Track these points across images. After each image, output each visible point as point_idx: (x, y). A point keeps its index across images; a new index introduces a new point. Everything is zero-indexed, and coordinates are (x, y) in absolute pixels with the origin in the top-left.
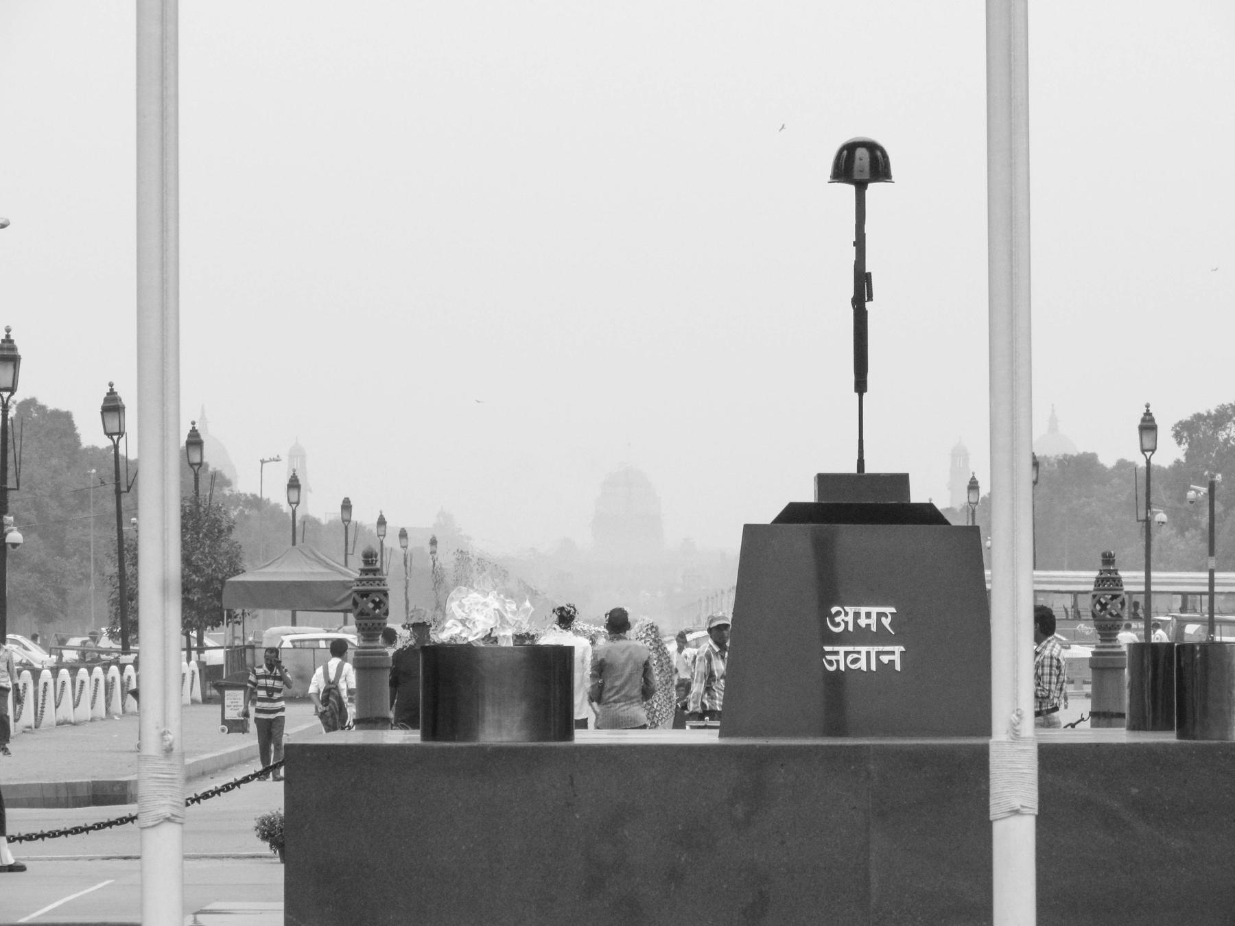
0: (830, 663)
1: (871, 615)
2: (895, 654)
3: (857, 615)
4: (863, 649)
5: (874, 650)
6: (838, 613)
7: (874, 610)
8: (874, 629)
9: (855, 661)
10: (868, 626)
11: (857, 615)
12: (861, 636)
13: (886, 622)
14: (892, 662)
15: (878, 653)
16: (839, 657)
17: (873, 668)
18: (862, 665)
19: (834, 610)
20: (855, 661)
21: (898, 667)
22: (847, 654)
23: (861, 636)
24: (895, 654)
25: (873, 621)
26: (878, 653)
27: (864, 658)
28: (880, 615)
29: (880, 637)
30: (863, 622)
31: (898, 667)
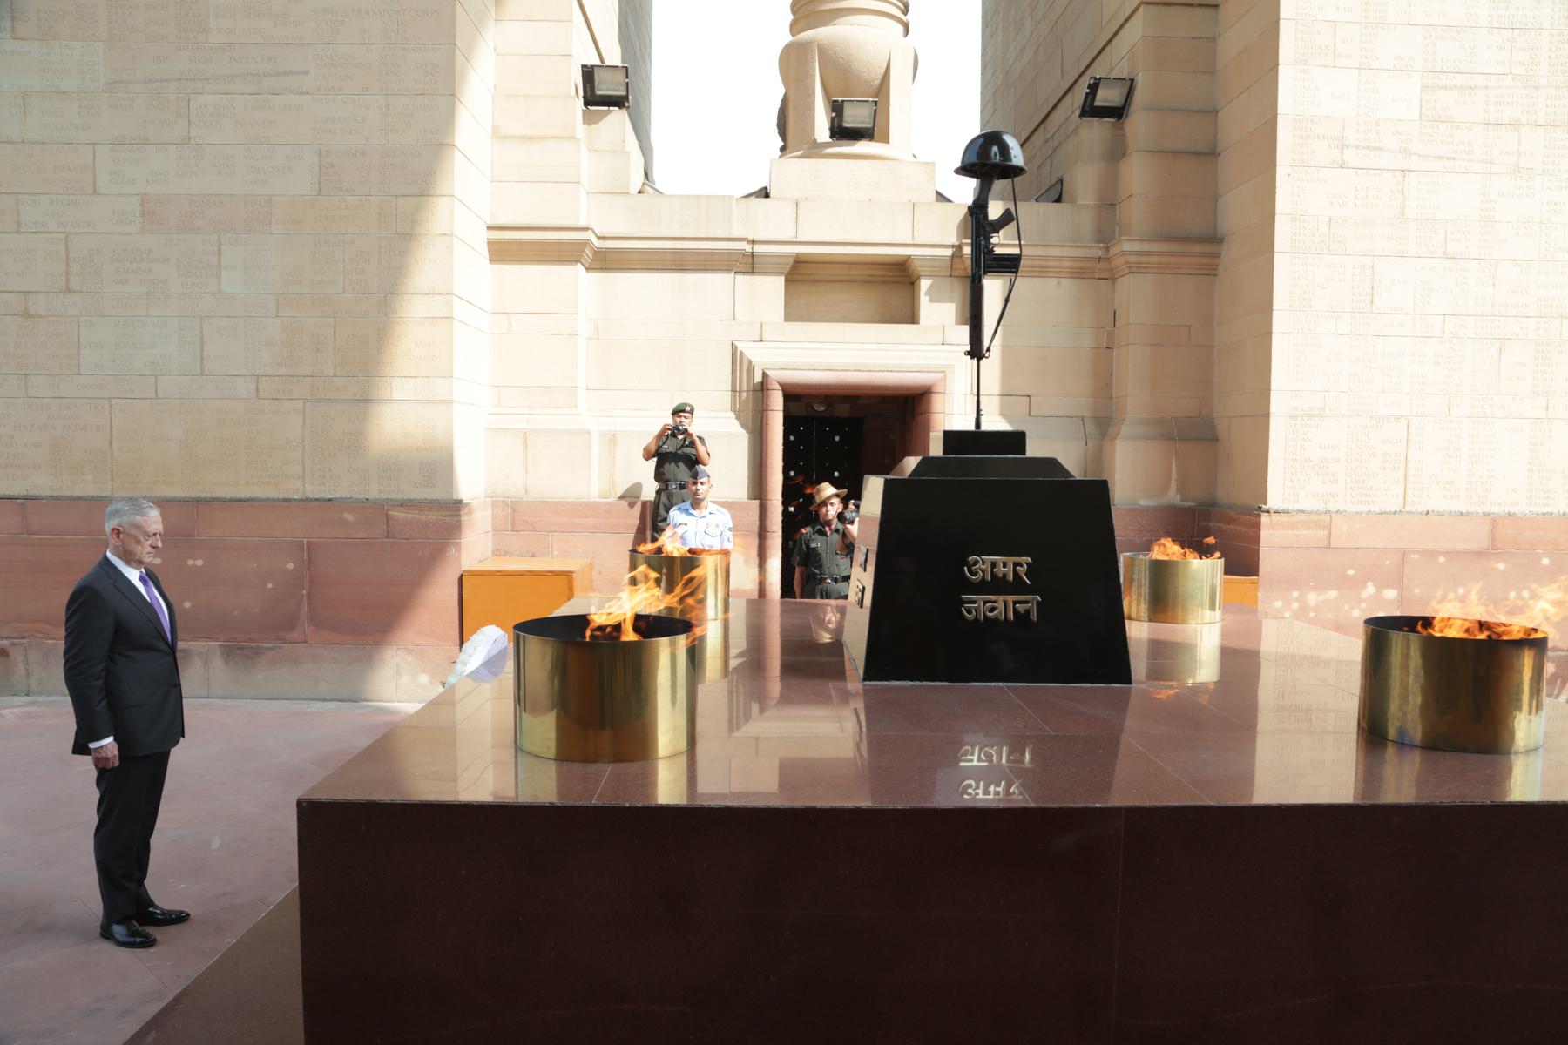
0: (969, 611)
1: (1007, 566)
2: (1030, 603)
3: (994, 565)
4: (1001, 598)
5: (1010, 598)
6: (976, 562)
7: (1011, 560)
8: (1011, 578)
9: (992, 609)
10: (1005, 575)
11: (994, 565)
12: (997, 585)
13: (1022, 570)
14: (1028, 611)
15: (1015, 603)
16: (978, 605)
17: (1011, 615)
18: (999, 612)
19: (972, 558)
20: (992, 609)
21: (1034, 616)
22: (985, 602)
23: (997, 585)
24: (1030, 603)
25: (1009, 570)
26: (1015, 603)
27: (1001, 606)
28: (1016, 564)
29: (1016, 586)
30: (1000, 570)
31: (1034, 616)
